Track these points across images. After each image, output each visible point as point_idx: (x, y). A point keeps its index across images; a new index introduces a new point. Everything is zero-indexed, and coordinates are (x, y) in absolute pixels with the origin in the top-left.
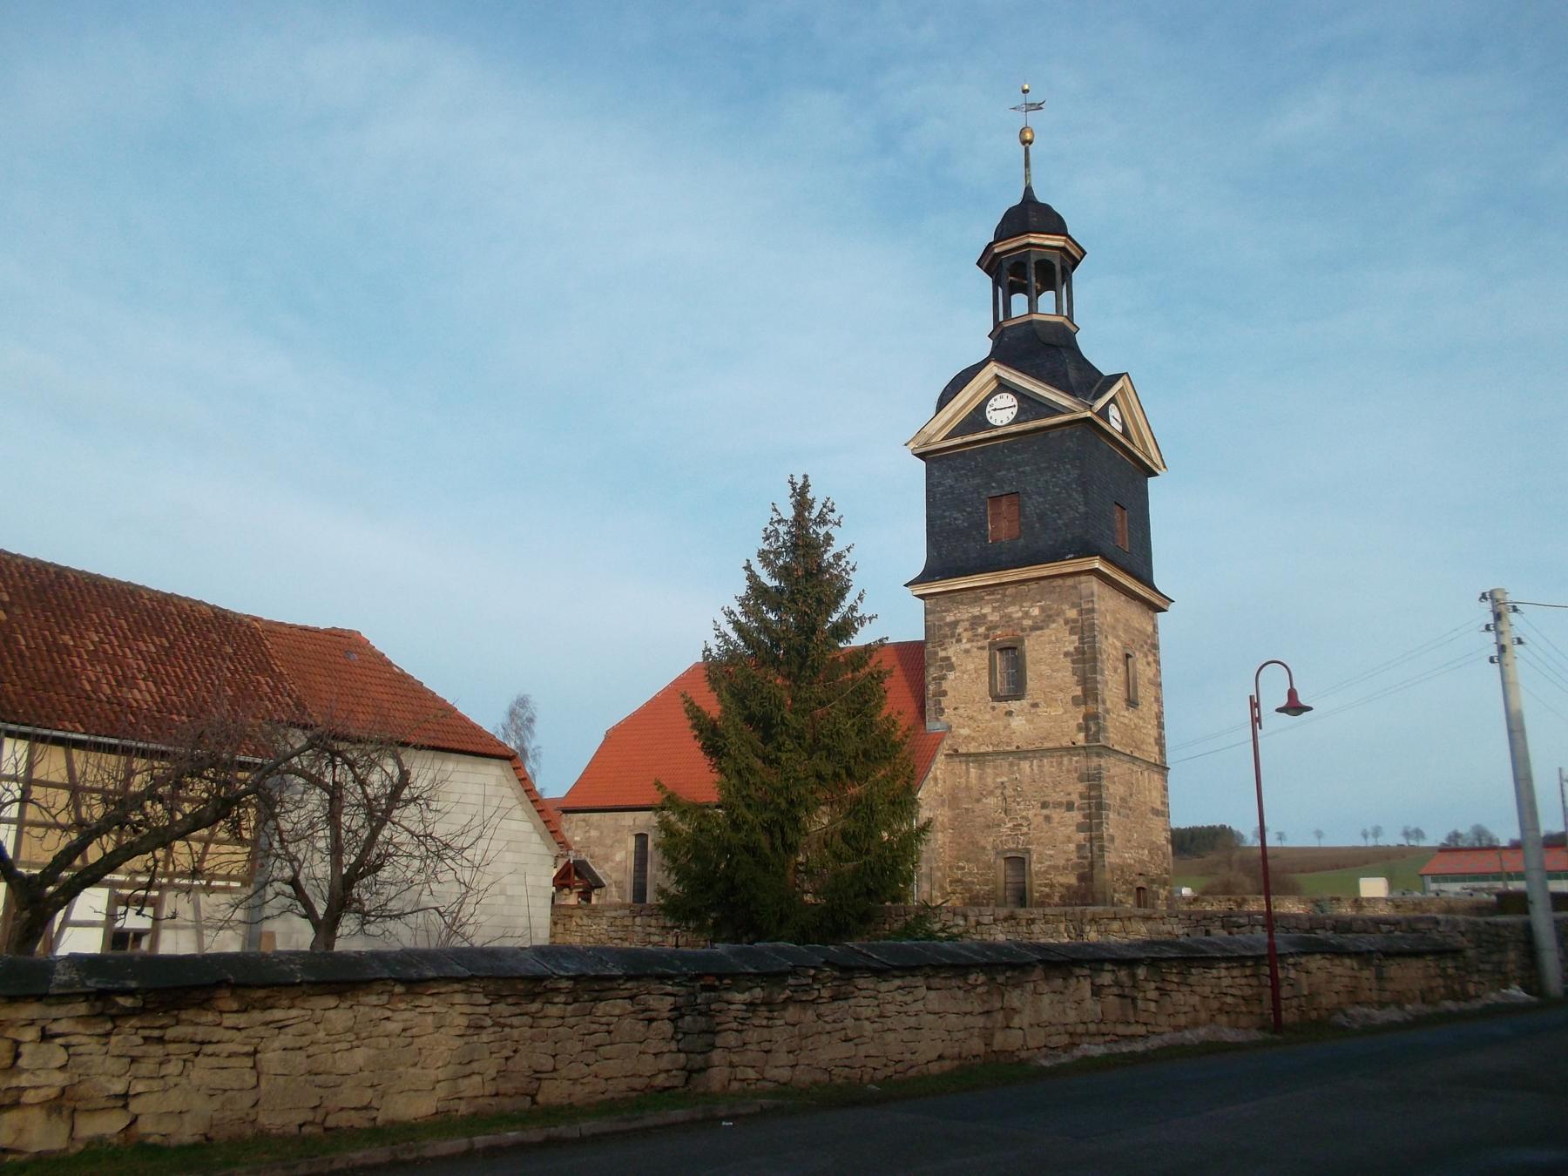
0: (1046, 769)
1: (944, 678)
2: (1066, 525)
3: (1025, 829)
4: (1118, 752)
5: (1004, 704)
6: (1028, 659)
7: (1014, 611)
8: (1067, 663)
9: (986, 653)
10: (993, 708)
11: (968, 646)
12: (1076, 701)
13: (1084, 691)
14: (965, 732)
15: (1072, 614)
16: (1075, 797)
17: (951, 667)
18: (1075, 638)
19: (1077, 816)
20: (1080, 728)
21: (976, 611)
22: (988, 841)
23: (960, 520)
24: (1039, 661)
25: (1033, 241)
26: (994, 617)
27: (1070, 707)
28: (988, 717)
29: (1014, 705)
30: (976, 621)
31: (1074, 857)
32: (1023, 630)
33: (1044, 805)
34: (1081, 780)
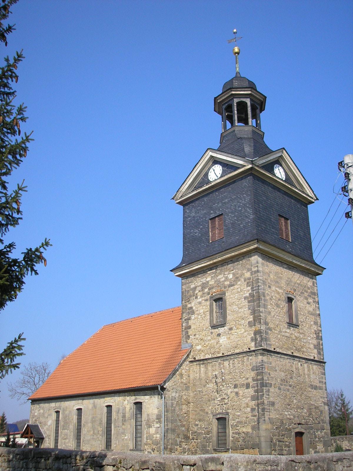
0: (236, 365)
1: (189, 319)
2: (244, 227)
3: (226, 401)
4: (279, 353)
5: (216, 330)
6: (228, 303)
7: (221, 277)
8: (245, 303)
9: (208, 303)
10: (212, 333)
11: (200, 300)
12: (250, 324)
13: (254, 318)
14: (199, 347)
15: (248, 275)
16: (250, 380)
17: (193, 313)
18: (249, 288)
19: (251, 392)
20: (252, 340)
21: (204, 280)
22: (209, 409)
23: (197, 233)
24: (232, 304)
25: (234, 92)
26: (212, 283)
27: (247, 328)
28: (209, 338)
29: (221, 330)
30: (204, 286)
31: (250, 415)
32: (225, 287)
33: (236, 386)
34: (253, 370)
